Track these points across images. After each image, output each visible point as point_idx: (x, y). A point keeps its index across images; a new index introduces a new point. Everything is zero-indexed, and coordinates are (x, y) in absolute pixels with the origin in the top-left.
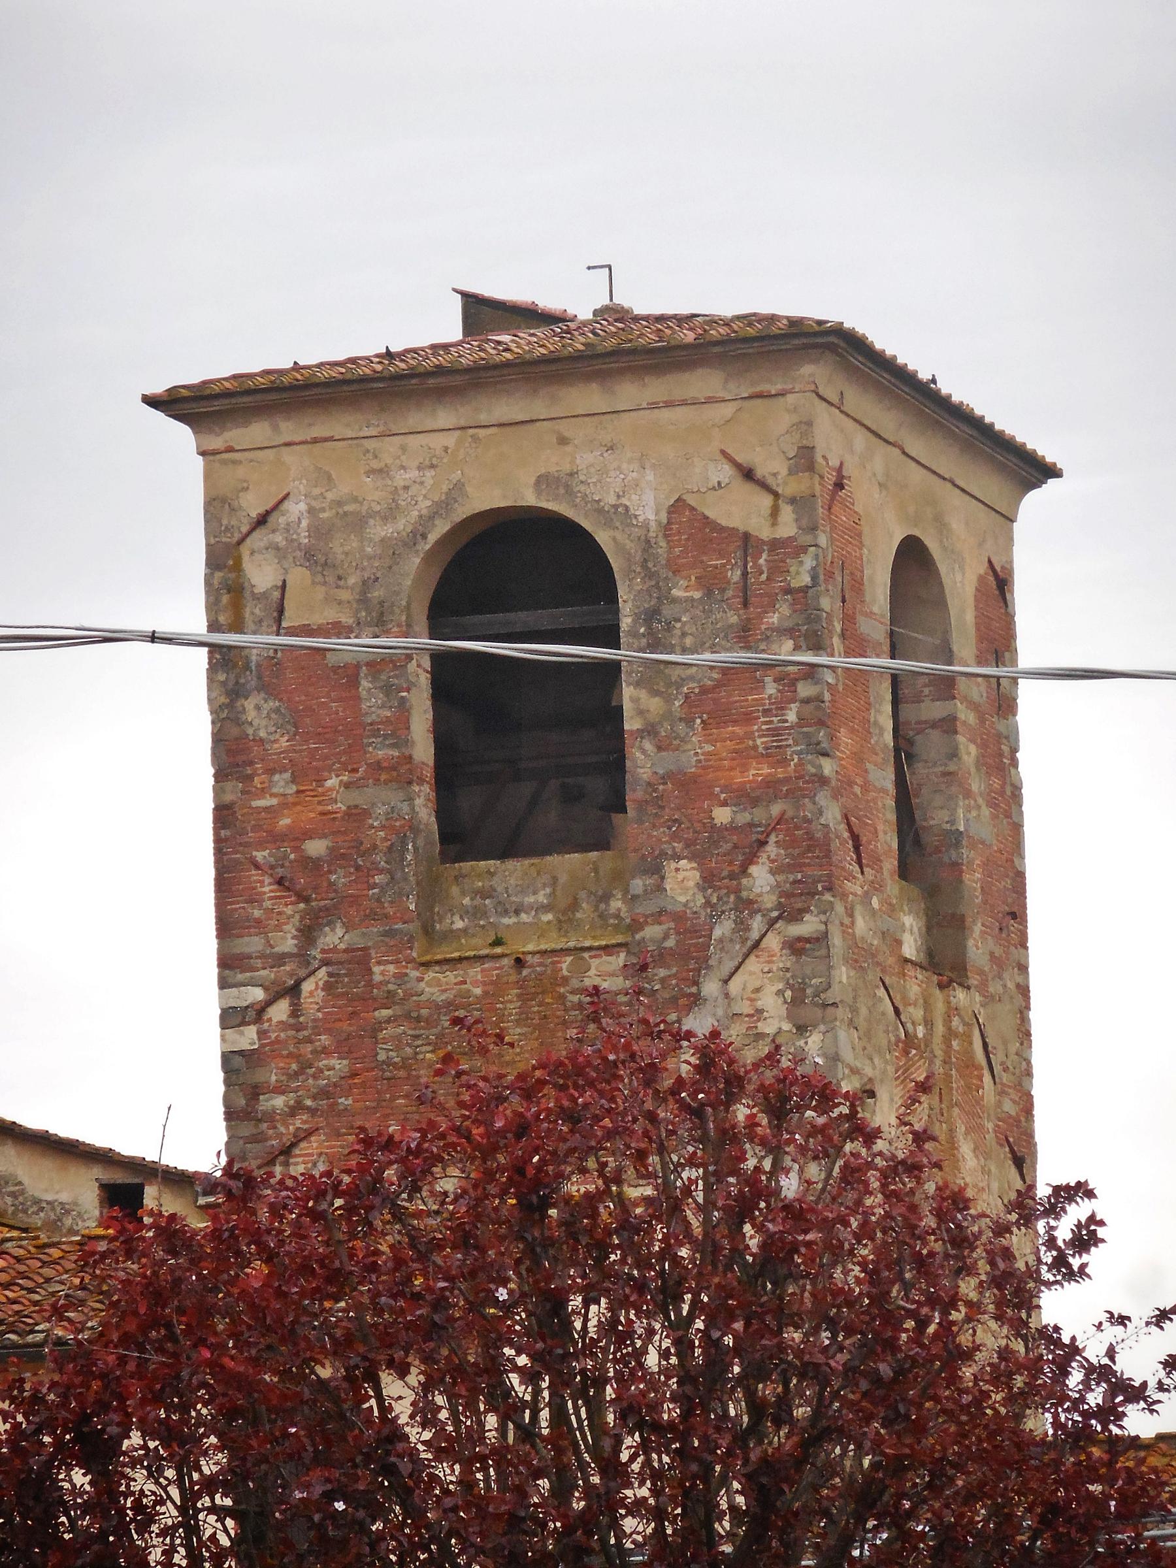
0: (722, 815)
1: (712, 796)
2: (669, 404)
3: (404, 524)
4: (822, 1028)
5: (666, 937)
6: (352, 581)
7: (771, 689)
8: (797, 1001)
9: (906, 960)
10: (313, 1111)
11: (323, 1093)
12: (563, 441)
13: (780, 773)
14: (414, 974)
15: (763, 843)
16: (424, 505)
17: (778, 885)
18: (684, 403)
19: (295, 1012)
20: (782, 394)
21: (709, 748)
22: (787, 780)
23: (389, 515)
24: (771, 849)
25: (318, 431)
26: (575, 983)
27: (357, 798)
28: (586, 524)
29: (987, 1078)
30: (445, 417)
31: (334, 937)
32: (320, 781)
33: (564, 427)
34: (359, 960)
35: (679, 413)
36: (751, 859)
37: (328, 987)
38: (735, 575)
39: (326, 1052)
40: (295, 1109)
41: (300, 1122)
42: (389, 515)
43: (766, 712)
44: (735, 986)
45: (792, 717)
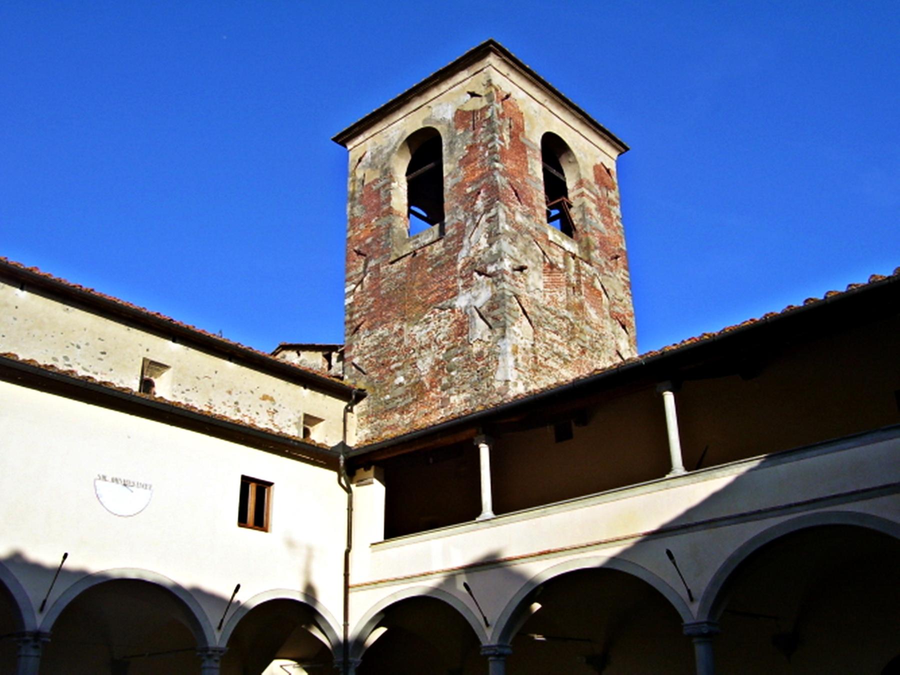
0: (469, 190)
1: (465, 185)
2: (454, 86)
3: (392, 147)
4: (497, 242)
5: (454, 232)
6: (380, 166)
7: (481, 149)
8: (490, 236)
9: (551, 242)
10: (365, 315)
11: (368, 309)
12: (430, 107)
13: (484, 171)
14: (390, 266)
15: (479, 193)
16: (396, 140)
17: (484, 204)
18: (458, 84)
19: (362, 288)
20: (482, 70)
21: (465, 173)
22: (486, 173)
23: (387, 147)
24: (482, 194)
25: (373, 133)
26: (430, 254)
27: (379, 223)
28: (434, 126)
29: (604, 296)
30: (400, 114)
31: (372, 263)
32: (370, 222)
33: (429, 104)
34: (377, 267)
35: (457, 87)
36: (476, 199)
37: (370, 278)
38: (471, 123)
39: (369, 297)
40: (360, 317)
41: (362, 320)
42: (387, 147)
43: (480, 156)
44: (472, 239)
45: (487, 154)
